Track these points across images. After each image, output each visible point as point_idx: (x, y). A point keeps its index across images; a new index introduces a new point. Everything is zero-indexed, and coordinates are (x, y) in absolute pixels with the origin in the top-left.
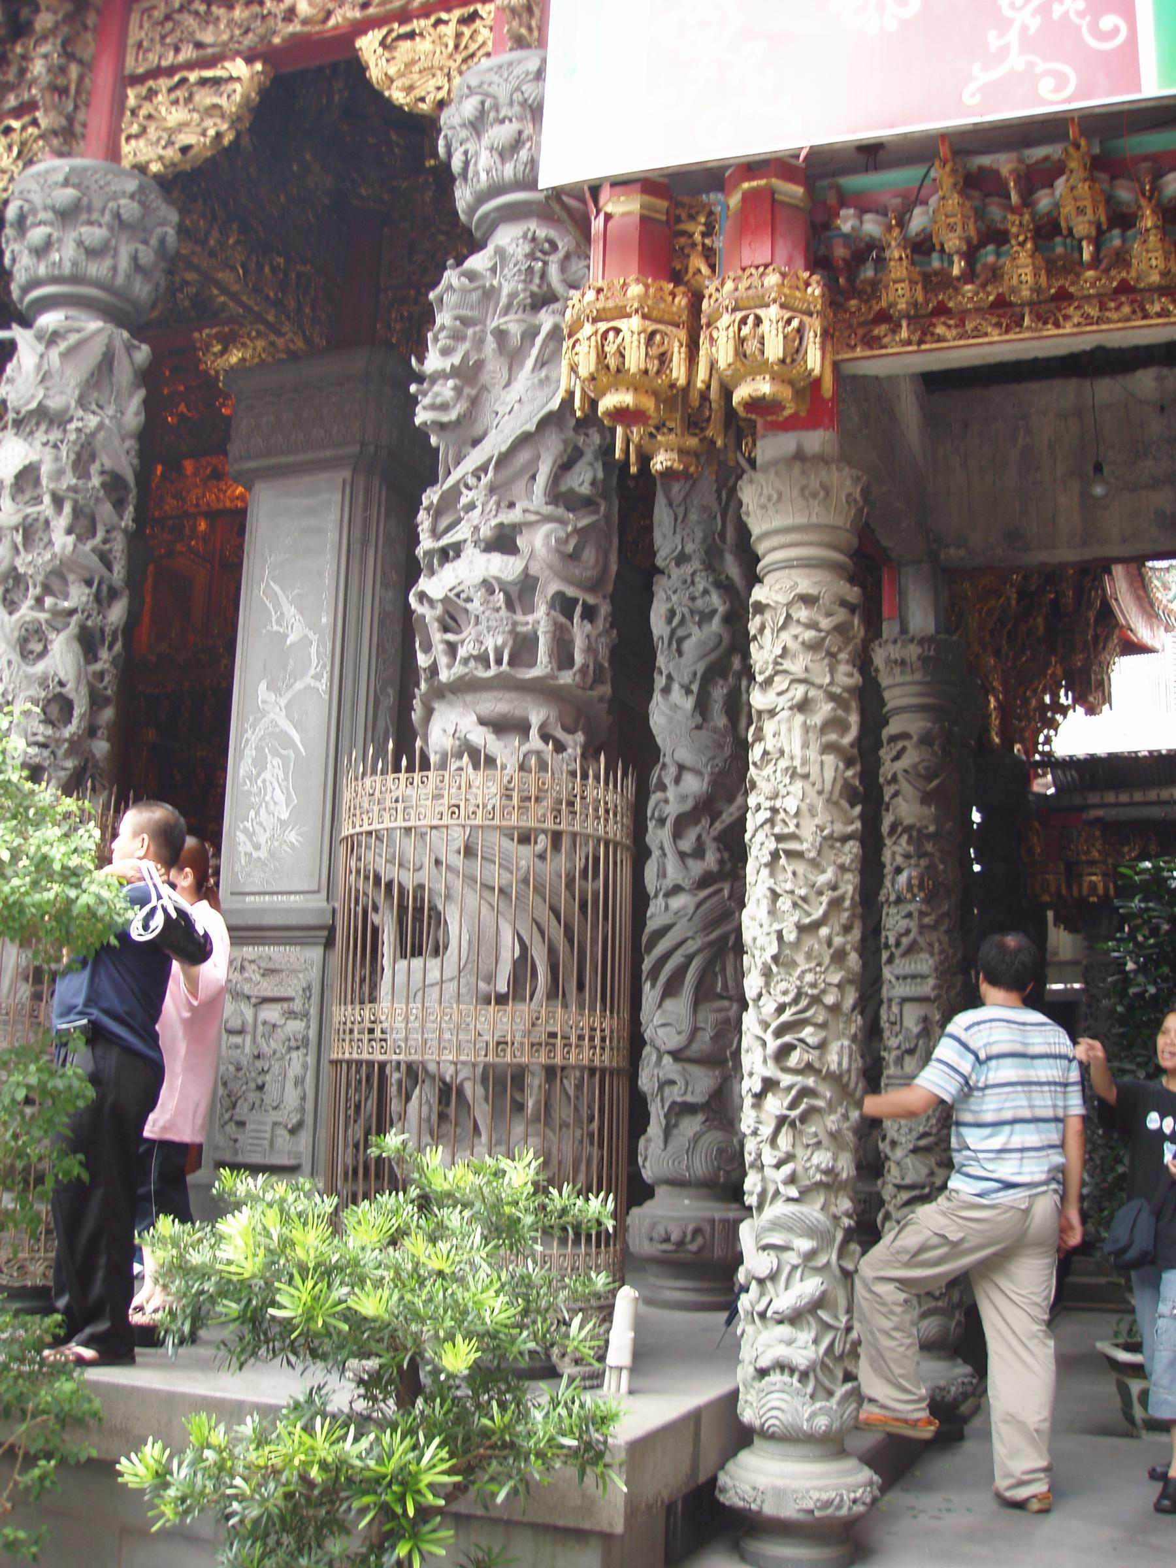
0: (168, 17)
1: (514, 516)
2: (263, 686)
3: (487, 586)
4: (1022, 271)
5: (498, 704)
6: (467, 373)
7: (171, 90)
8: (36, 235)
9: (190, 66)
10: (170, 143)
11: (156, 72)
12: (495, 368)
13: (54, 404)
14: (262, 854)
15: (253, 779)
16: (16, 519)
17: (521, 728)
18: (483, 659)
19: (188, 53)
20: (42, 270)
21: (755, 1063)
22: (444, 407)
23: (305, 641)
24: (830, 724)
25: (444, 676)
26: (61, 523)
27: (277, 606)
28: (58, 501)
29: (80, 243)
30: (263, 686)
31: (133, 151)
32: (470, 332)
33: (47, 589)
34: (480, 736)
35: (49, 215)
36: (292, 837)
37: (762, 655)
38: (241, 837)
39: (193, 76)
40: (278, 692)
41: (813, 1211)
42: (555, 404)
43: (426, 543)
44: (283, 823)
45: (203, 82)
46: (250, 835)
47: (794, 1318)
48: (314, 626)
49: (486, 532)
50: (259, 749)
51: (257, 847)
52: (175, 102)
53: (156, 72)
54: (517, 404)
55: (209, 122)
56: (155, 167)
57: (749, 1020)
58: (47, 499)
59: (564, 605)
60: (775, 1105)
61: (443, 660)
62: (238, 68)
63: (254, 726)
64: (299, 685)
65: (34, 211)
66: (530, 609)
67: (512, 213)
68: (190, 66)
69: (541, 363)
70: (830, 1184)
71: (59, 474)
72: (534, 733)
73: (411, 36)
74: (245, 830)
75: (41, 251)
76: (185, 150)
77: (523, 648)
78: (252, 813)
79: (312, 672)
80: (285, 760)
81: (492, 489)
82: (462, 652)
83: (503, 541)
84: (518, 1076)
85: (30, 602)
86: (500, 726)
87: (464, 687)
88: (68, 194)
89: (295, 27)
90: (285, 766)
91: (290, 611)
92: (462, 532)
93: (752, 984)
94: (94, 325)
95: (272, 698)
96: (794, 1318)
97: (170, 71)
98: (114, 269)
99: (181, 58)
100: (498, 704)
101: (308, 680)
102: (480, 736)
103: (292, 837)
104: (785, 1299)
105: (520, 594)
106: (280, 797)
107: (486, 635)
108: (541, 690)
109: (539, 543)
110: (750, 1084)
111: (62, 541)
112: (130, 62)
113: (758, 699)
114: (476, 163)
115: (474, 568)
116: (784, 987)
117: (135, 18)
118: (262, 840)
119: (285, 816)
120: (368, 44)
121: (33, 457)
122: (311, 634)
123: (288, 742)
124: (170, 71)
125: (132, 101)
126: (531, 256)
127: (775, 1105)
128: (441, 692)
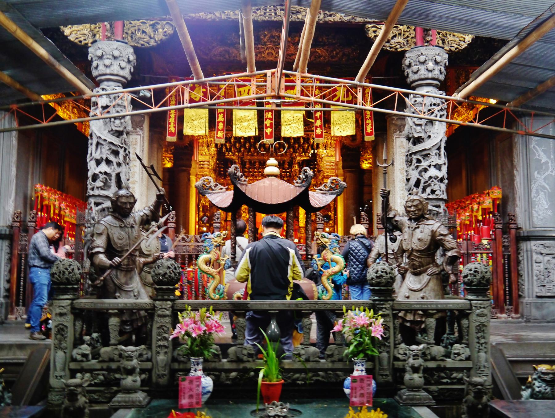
2: (536, 173)
15: (536, 197)
23: (547, 163)
27: (537, 151)
30: (536, 173)
36: (549, 213)
38: (534, 212)
40: (541, 175)
44: (546, 209)
46: (537, 212)
48: (549, 157)
50: (537, 190)
51: (539, 215)
63: (534, 183)
64: (546, 174)
74: (535, 211)
78: (537, 206)
79: (550, 170)
80: (545, 193)
90: (545, 194)
91: (542, 154)
95: (539, 176)
101: (549, 172)
103: (549, 213)
106: (545, 203)
118: (541, 213)
119: (547, 207)
122: (548, 160)
123: (544, 188)
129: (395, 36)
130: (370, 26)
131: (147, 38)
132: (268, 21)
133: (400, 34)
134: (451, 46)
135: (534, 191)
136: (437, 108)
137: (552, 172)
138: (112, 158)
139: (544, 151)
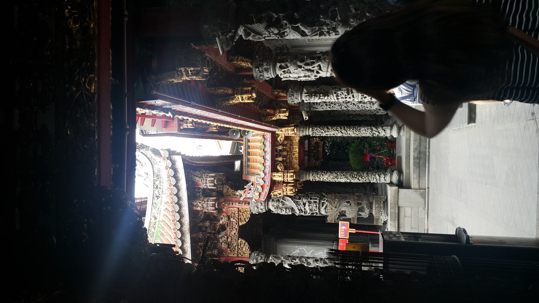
1: (302, 203)
4: (285, 153)
5: (321, 205)
12: (285, 206)
17: (323, 203)
19: (236, 248)
21: (356, 181)
24: (324, 173)
26: (294, 261)
34: (324, 207)
37: (317, 179)
41: (370, 175)
42: (290, 199)
43: (303, 214)
47: (380, 177)
48: (297, 249)
57: (352, 181)
59: (311, 199)
60: (360, 179)
62: (240, 241)
67: (268, 205)
70: (367, 174)
77: (315, 202)
83: (304, 204)
84: (358, 203)
86: (323, 206)
89: (237, 234)
92: (303, 209)
93: (348, 181)
94: (270, 258)
96: (380, 177)
100: (321, 205)
102: (324, 207)
104: (378, 178)
108: (320, 201)
109: (305, 201)
110: (358, 181)
113: (321, 180)
114: (262, 209)
116: (349, 177)
120: (241, 224)
127: (360, 179)
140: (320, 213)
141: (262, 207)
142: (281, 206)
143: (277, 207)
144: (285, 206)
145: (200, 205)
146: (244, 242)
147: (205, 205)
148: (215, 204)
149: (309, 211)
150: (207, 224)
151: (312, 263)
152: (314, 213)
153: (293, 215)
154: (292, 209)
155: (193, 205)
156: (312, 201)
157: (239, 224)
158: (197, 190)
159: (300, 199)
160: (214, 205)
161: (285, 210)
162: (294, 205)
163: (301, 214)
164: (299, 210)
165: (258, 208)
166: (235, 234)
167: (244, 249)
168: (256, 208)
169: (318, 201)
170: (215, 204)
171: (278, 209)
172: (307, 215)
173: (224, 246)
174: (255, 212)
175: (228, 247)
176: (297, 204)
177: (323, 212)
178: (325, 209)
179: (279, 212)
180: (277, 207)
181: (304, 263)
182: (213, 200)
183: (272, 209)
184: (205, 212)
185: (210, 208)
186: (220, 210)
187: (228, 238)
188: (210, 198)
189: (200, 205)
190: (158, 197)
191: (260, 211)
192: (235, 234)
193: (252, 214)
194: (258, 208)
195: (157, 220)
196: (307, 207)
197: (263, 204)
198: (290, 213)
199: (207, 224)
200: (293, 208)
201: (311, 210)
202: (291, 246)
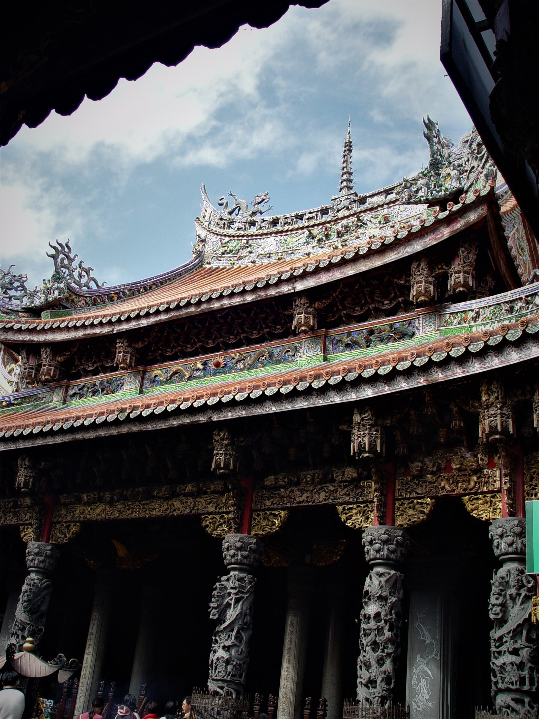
0: (407, 483)
1: (517, 646)
2: (418, 656)
3: (512, 663)
6: (503, 605)
7: (409, 504)
8: (377, 546)
9: (415, 498)
10: (410, 520)
11: (405, 499)
12: (510, 603)
13: (384, 594)
14: (421, 709)
16: (375, 627)
18: (512, 683)
19: (414, 495)
20: (378, 556)
22: (498, 614)
23: (431, 644)
25: (500, 685)
28: (386, 622)
29: (388, 550)
31: (399, 521)
32: (503, 593)
33: (384, 648)
35: (379, 541)
39: (415, 501)
40: (424, 658)
43: (493, 649)
45: (418, 503)
48: (433, 638)
49: (510, 649)
52: (410, 508)
53: (405, 499)
54: (516, 615)
55: (420, 515)
56: (405, 526)
58: (383, 621)
61: (500, 681)
63: (416, 668)
65: (375, 540)
66: (523, 670)
68: (415, 498)
69: (522, 603)
71: (386, 615)
72: (526, 705)
73: (477, 499)
75: (378, 551)
76: (414, 522)
77: (522, 680)
79: (434, 653)
81: (512, 638)
82: (506, 680)
83: (515, 652)
85: (380, 650)
87: (507, 690)
88: (385, 536)
92: (503, 648)
94: (393, 572)
97: (409, 499)
98: (397, 556)
99: (411, 496)
105: (521, 666)
107: (512, 676)
109: (525, 653)
111: (388, 634)
112: (397, 494)
115: (508, 658)
117: (397, 481)
121: (379, 610)
122: (433, 641)
124: (409, 499)
125: (397, 505)
126: (518, 575)
128: (500, 691)
129: (221, 525)
130: (203, 516)
131: (63, 536)
132: (134, 518)
133: (224, 523)
134: (263, 531)
135: (415, 676)
136: (232, 591)
137: (436, 655)
138: (19, 633)
139: (429, 631)
140: (496, 694)
141: (503, 546)
142: (509, 592)
143: (505, 584)
144: (510, 603)
145: (492, 399)
146: (426, 511)
147: (492, 411)
148: (497, 433)
149: (499, 661)
150: (456, 424)
151: (383, 668)
152: (495, 676)
153: (491, 625)
154: (503, 621)
155: (489, 384)
156: (526, 673)
157: (465, 495)
158: (528, 388)
159: (529, 639)
160: (493, 430)
161: (499, 601)
162: (511, 625)
163: (493, 644)
164: (501, 638)
165: (501, 536)
166: (443, 488)
167: (411, 512)
168: (499, 531)
169: (526, 688)
170: (497, 433)
171: (500, 584)
172: (494, 660)
173: (415, 467)
174: (494, 531)
175: (414, 477)
176: (516, 633)
177: (501, 700)
178: (508, 707)
179: (495, 589)
180: (505, 584)
181: (383, 651)
182: (505, 428)
183: (502, 572)
184: (478, 414)
185: (487, 422)
186: (491, 449)
187: (433, 473)
188: (510, 422)
189: (492, 399)
190: (511, 310)
191: (495, 543)
192: (443, 488)
193: (488, 523)
194: (501, 536)
195: (472, 323)
196: (508, 658)
197: (510, 549)
198: (492, 616)
199: (456, 424)
200: (506, 622)
201: (503, 667)
202: (438, 624)
